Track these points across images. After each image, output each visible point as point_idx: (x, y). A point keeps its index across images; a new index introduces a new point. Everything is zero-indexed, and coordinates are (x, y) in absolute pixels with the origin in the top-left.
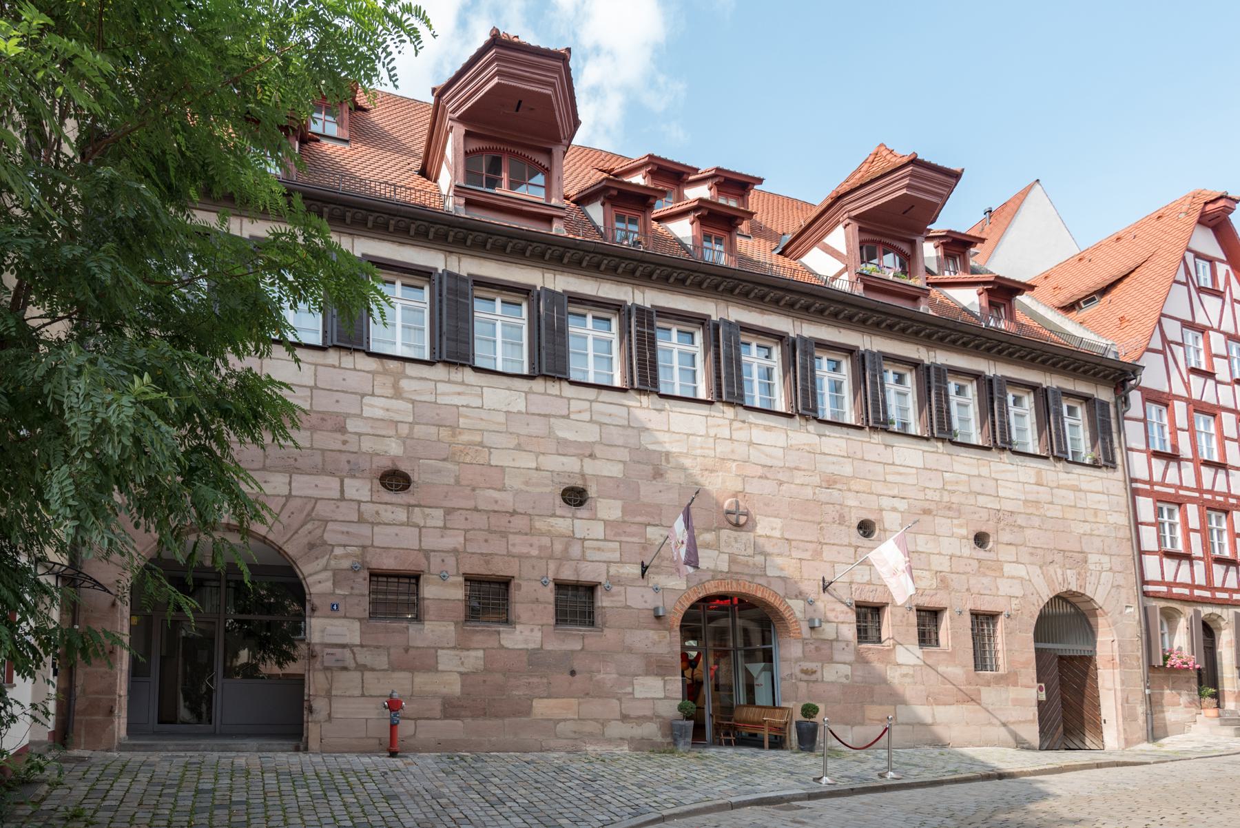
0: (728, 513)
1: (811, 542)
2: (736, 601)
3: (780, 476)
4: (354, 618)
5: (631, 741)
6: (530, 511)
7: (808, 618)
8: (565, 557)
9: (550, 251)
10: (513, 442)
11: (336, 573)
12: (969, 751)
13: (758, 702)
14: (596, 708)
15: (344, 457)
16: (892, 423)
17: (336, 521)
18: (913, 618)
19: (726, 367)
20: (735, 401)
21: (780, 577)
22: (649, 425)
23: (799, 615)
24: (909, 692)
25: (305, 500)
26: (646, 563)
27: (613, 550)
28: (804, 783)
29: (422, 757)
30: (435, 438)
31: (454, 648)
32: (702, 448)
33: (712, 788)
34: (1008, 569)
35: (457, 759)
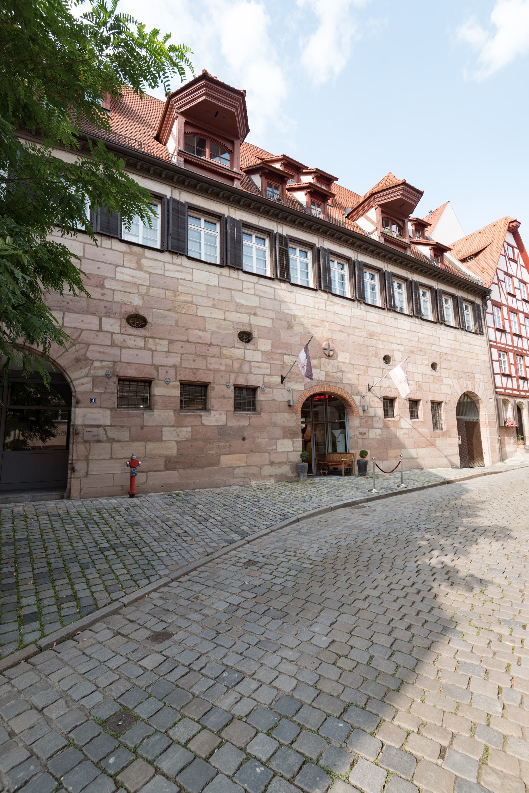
0: (325, 349)
1: (363, 366)
2: (327, 396)
3: (350, 331)
4: (107, 408)
5: (275, 476)
6: (220, 344)
7: (362, 405)
8: (240, 372)
9: (233, 197)
10: (211, 303)
11: (94, 378)
12: (433, 471)
13: (338, 451)
14: (256, 458)
15: (102, 304)
16: (397, 308)
17: (96, 344)
18: (407, 405)
19: (323, 272)
20: (328, 290)
21: (349, 384)
22: (285, 300)
23: (358, 404)
24: (407, 442)
25: (74, 330)
26: (284, 376)
27: (266, 368)
28: (364, 493)
29: (151, 496)
30: (163, 297)
31: (173, 426)
32: (312, 314)
33: (321, 500)
34: (445, 380)
35: (174, 495)
